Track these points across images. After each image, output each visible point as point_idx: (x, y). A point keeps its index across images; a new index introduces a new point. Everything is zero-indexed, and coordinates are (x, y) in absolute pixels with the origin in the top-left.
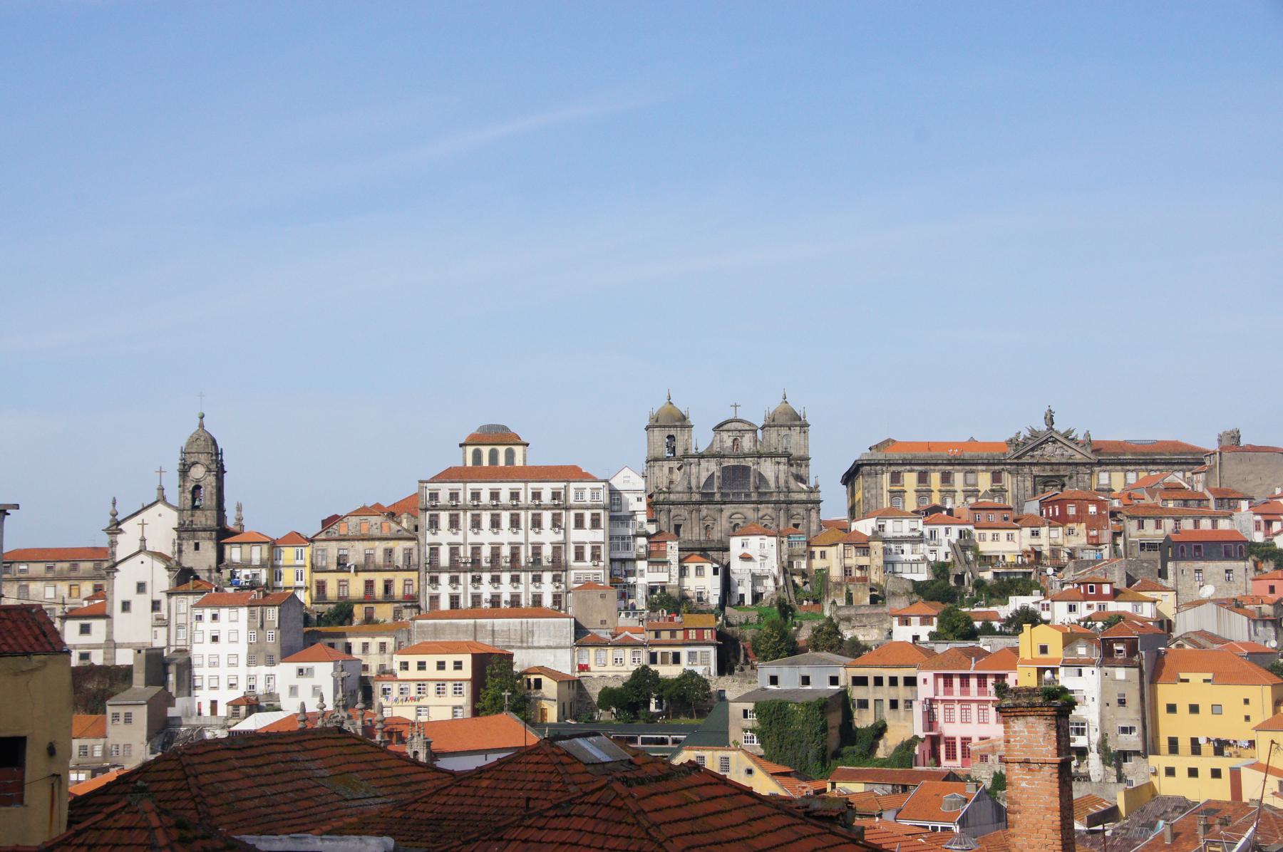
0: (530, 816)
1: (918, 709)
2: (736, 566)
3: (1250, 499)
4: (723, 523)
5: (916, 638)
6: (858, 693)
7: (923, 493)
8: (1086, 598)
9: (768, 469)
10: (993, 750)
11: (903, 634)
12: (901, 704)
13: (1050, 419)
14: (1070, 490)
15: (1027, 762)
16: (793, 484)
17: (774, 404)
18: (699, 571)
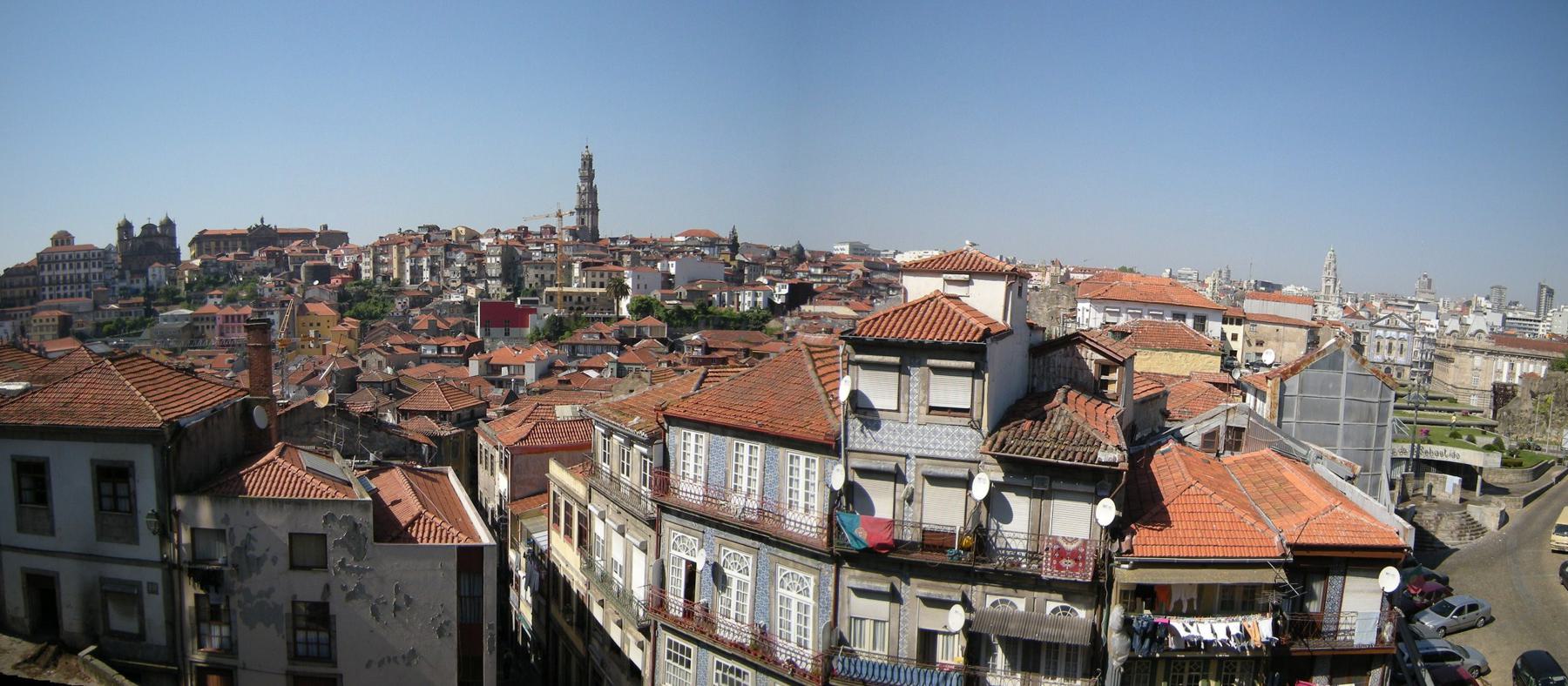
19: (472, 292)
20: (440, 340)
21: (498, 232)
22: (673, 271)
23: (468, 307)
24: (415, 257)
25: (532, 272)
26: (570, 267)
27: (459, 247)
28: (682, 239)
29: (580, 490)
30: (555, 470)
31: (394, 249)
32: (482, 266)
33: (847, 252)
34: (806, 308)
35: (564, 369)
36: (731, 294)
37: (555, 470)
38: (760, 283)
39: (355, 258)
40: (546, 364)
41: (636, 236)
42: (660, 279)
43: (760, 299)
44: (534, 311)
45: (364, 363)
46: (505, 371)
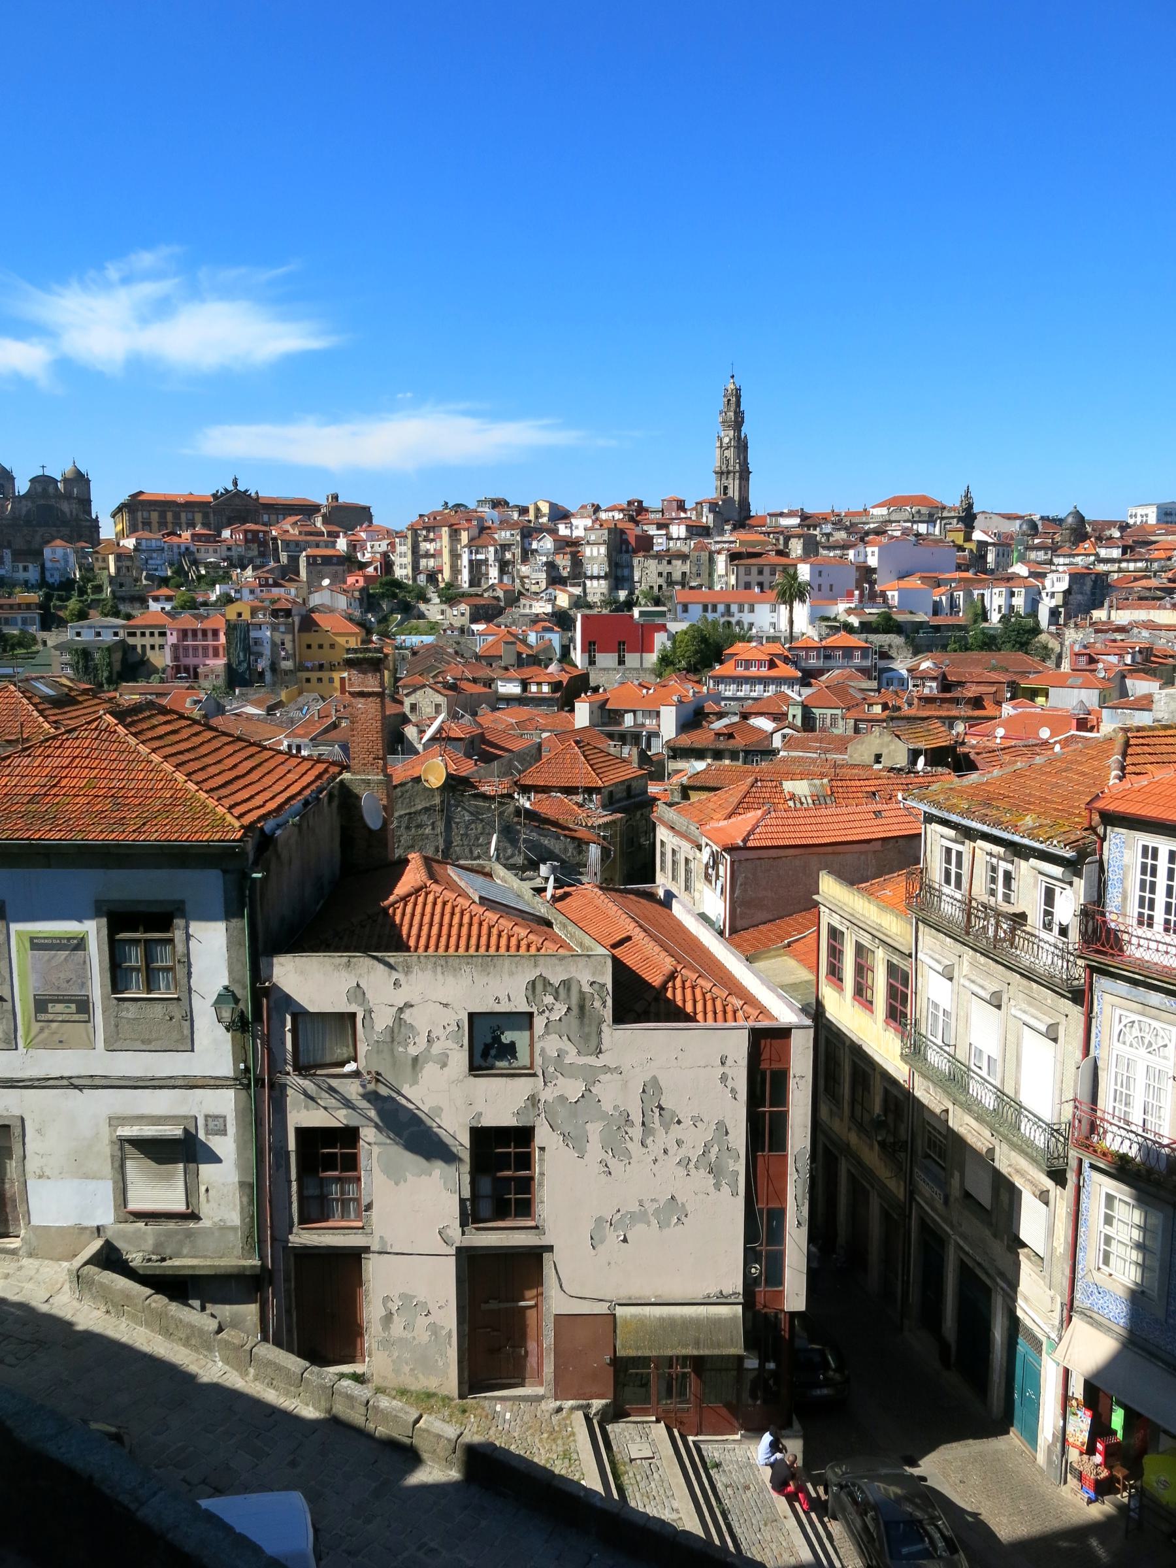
0: (47, 740)
1: (167, 650)
2: (48, 565)
3: (345, 533)
4: (38, 538)
5: (163, 609)
6: (131, 641)
7: (163, 524)
8: (261, 586)
9: (65, 507)
10: (212, 671)
11: (154, 606)
12: (157, 647)
13: (235, 484)
14: (250, 526)
15: (362, 694)
16: (82, 516)
17: (68, 468)
18: (25, 569)
19: (563, 601)
20: (527, 672)
21: (597, 509)
22: (873, 562)
23: (562, 620)
24: (475, 545)
25: (653, 566)
26: (711, 561)
27: (541, 530)
28: (883, 511)
29: (896, 927)
30: (829, 887)
31: (445, 531)
32: (577, 563)
33: (1152, 520)
34: (1099, 615)
35: (721, 715)
36: (969, 595)
37: (829, 887)
38: (1019, 577)
39: (383, 546)
40: (690, 709)
41: (809, 510)
42: (853, 575)
43: (1019, 601)
44: (663, 628)
45: (413, 707)
46: (629, 720)
